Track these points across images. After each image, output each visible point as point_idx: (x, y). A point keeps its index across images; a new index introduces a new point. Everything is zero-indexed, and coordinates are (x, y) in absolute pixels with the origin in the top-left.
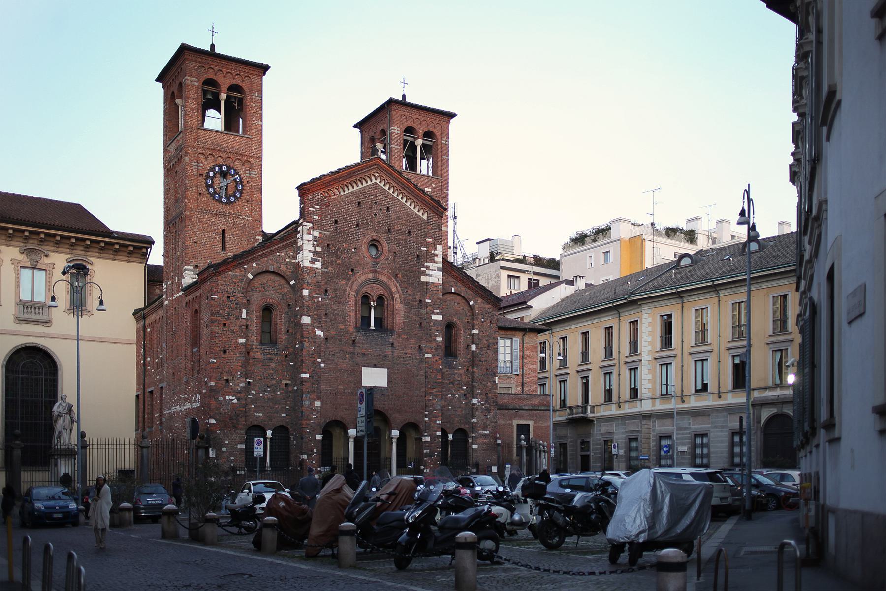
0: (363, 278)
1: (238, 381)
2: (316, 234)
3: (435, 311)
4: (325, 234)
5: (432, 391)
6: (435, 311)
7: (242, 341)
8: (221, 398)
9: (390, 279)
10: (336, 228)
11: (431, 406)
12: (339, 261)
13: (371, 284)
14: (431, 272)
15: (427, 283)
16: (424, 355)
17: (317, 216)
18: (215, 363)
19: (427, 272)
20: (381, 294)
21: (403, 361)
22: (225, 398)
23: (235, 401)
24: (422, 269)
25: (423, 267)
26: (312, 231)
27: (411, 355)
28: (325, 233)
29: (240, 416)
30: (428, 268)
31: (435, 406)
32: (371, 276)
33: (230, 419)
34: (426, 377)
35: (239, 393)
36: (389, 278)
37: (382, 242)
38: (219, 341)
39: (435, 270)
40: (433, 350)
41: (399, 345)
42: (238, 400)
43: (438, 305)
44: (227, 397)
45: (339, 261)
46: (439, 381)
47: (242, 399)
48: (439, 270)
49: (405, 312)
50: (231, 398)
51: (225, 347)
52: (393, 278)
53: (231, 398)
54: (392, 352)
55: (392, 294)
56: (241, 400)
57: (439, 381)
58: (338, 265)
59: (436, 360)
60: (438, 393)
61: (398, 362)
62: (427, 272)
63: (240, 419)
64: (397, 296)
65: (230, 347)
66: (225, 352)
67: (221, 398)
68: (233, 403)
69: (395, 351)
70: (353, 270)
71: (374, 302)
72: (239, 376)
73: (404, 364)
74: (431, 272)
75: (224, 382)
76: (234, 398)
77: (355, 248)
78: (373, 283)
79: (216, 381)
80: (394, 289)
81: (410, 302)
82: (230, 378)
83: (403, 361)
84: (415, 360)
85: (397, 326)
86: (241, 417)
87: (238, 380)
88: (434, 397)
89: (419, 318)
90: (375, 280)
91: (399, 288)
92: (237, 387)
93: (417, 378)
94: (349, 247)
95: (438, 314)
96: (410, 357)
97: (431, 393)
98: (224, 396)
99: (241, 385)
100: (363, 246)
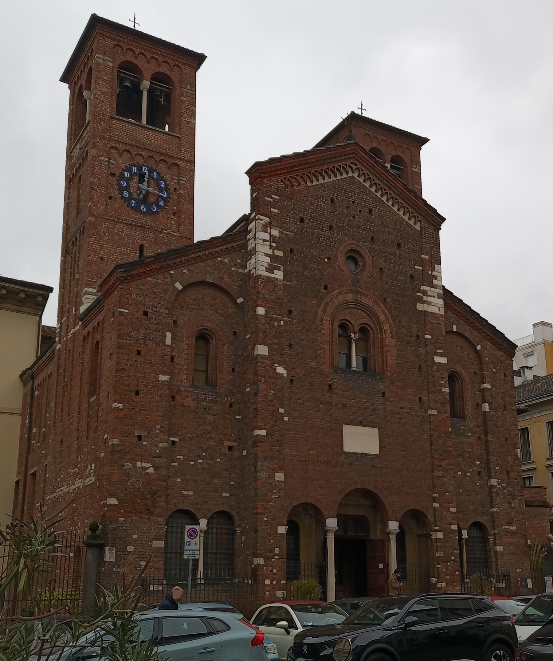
0: (340, 299)
1: (155, 439)
2: (275, 232)
3: (438, 351)
4: (287, 235)
5: (440, 464)
6: (438, 351)
7: (164, 378)
8: (129, 465)
9: (377, 304)
10: (302, 229)
11: (441, 485)
12: (307, 273)
13: (350, 308)
14: (430, 299)
15: (425, 313)
16: (427, 411)
17: (276, 208)
18: (121, 410)
19: (425, 298)
20: (365, 324)
21: (398, 418)
22: (135, 466)
23: (151, 470)
24: (418, 294)
25: (420, 291)
26: (269, 229)
27: (409, 411)
28: (287, 233)
29: (158, 494)
30: (425, 293)
31: (447, 485)
32: (350, 297)
33: (141, 500)
34: (432, 443)
35: (158, 457)
36: (374, 301)
37: (364, 254)
38: (129, 376)
39: (435, 297)
40: (439, 405)
41: (393, 395)
42: (156, 468)
43: (441, 343)
44: (139, 464)
45: (307, 273)
46: (449, 449)
47: (162, 467)
48: (439, 297)
49: (398, 350)
50: (144, 465)
51: (138, 385)
52: (380, 302)
53: (144, 465)
54: (384, 405)
55: (379, 323)
56: (160, 469)
57: (449, 449)
58: (306, 278)
59: (444, 419)
60: (449, 467)
61: (393, 420)
62: (425, 298)
63: (158, 499)
64: (386, 326)
65: (146, 386)
66: (137, 393)
67: (129, 465)
68: (148, 474)
69: (388, 403)
70: (326, 288)
71: (355, 333)
72: (158, 431)
73: (400, 423)
74: (430, 299)
75: (135, 440)
76: (149, 465)
77: (329, 259)
78: (354, 308)
79: (121, 438)
80: (382, 318)
81: (405, 337)
82: (143, 434)
83: (398, 418)
84: (415, 418)
85: (389, 369)
86: (160, 496)
87: (156, 437)
88: (444, 473)
89: (417, 360)
90: (357, 304)
91: (389, 317)
92: (155, 448)
93: (420, 443)
94: (320, 255)
95: (441, 355)
96: (408, 413)
97: (440, 466)
98: (133, 461)
99: (161, 445)
100: (339, 255)
